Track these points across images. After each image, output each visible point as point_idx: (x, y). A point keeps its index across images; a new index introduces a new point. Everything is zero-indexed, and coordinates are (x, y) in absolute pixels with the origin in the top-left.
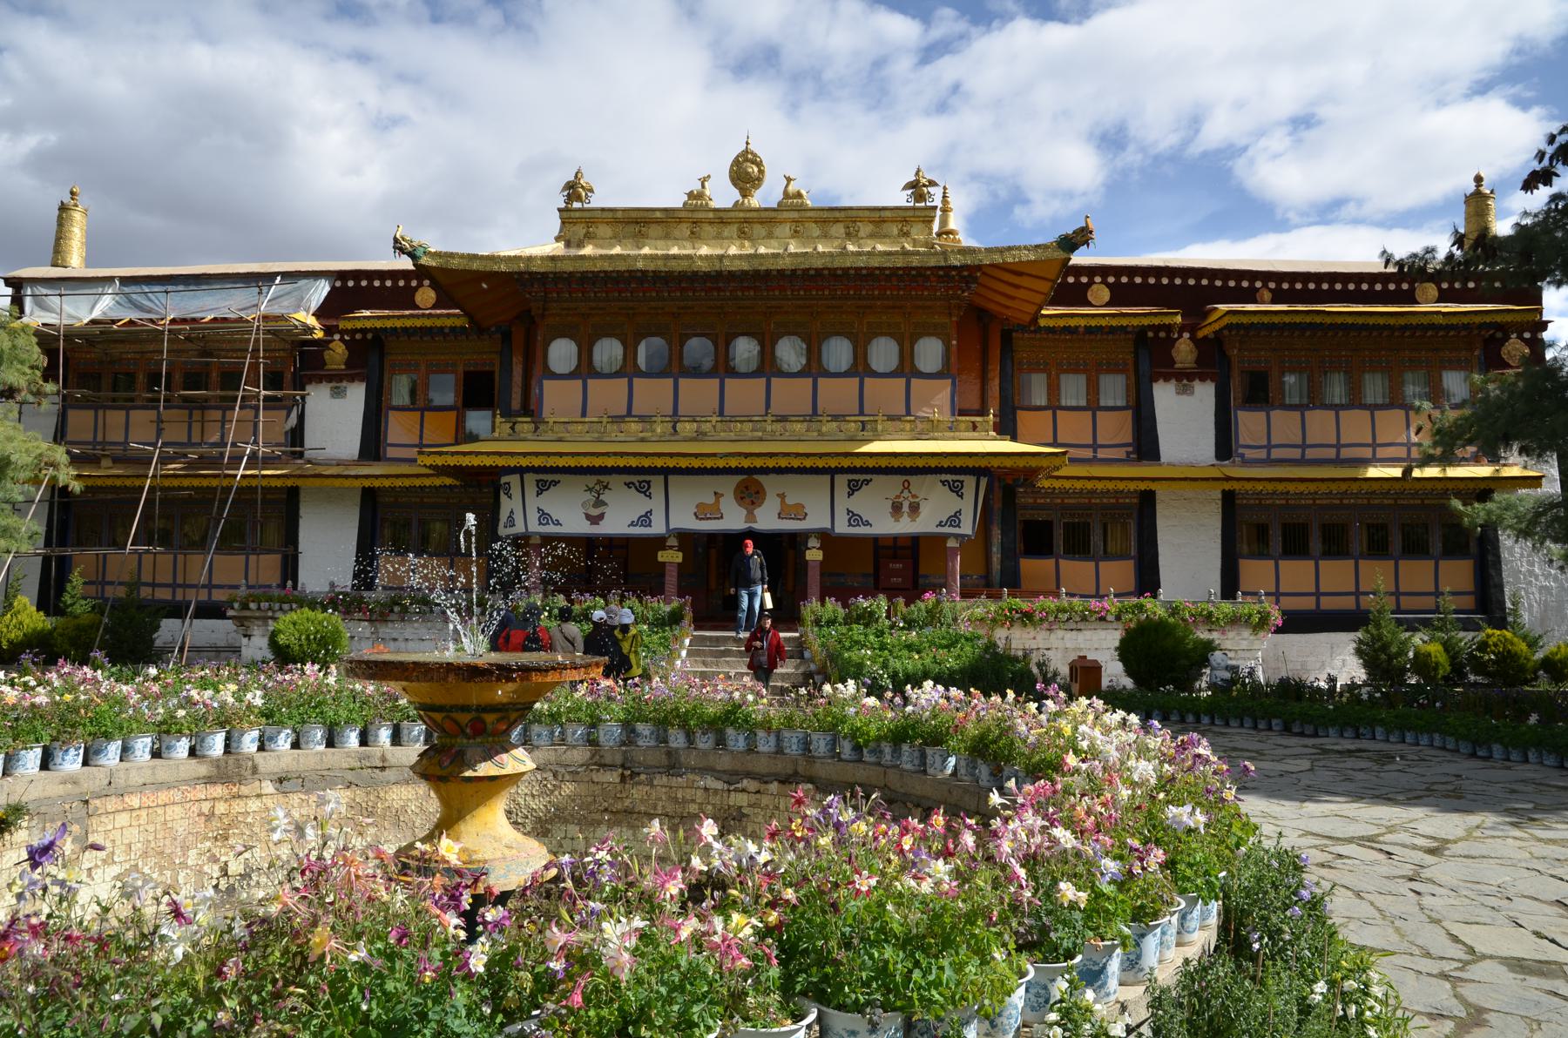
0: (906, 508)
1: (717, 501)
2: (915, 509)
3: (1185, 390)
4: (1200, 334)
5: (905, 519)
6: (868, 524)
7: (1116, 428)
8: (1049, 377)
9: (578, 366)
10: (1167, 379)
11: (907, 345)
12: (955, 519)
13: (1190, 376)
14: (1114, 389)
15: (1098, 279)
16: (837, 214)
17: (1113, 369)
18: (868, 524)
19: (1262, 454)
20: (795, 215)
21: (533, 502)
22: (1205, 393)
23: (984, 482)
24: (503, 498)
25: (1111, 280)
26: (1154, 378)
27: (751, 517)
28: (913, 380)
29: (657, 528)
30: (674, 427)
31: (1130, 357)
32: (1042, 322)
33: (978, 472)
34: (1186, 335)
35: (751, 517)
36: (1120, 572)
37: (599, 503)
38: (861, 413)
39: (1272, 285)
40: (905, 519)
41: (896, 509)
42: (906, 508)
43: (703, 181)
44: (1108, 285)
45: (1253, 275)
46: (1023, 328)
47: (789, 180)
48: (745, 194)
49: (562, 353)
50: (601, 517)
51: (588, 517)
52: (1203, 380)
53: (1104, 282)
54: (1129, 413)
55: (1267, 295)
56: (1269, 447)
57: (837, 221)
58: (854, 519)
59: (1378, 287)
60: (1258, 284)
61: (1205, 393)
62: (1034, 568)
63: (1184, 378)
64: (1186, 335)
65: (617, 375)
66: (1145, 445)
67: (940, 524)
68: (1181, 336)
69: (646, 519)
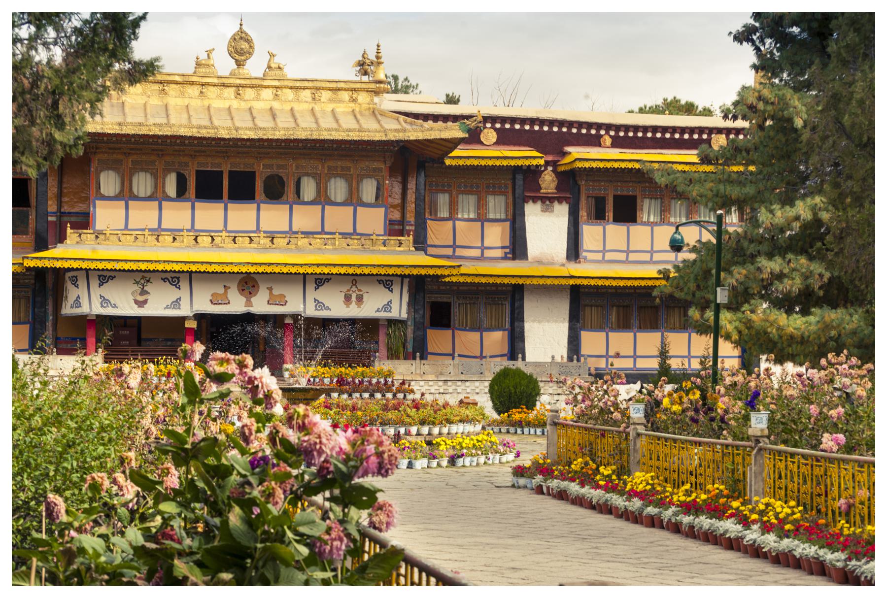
0: (354, 298)
1: (226, 292)
2: (360, 299)
3: (547, 209)
4: (561, 169)
5: (353, 305)
6: (328, 308)
7: (496, 235)
8: (451, 196)
9: (122, 191)
10: (535, 200)
11: (355, 184)
12: (388, 307)
13: (551, 200)
14: (496, 206)
15: (489, 125)
16: (306, 84)
17: (496, 191)
18: (328, 308)
19: (599, 256)
20: (276, 83)
21: (96, 292)
22: (561, 212)
23: (406, 281)
24: (69, 285)
25: (498, 126)
26: (525, 200)
27: (249, 303)
28: (358, 208)
29: (185, 311)
30: (196, 239)
31: (510, 183)
32: (448, 162)
33: (403, 277)
34: (550, 168)
35: (249, 303)
36: (496, 339)
37: (144, 292)
38: (323, 232)
39: (612, 133)
40: (353, 305)
41: (348, 299)
42: (354, 298)
43: (209, 53)
44: (496, 130)
45: (599, 126)
46: (433, 160)
47: (272, 55)
48: (239, 64)
49: (109, 182)
50: (145, 302)
51: (136, 302)
52: (560, 202)
53: (493, 127)
54: (508, 224)
55: (608, 141)
56: (604, 251)
57: (304, 88)
58: (319, 304)
59: (686, 136)
60: (602, 132)
61: (561, 212)
62: (437, 339)
63: (547, 201)
64: (550, 168)
65: (150, 198)
66: (517, 247)
67: (378, 311)
68: (546, 169)
69: (177, 303)
